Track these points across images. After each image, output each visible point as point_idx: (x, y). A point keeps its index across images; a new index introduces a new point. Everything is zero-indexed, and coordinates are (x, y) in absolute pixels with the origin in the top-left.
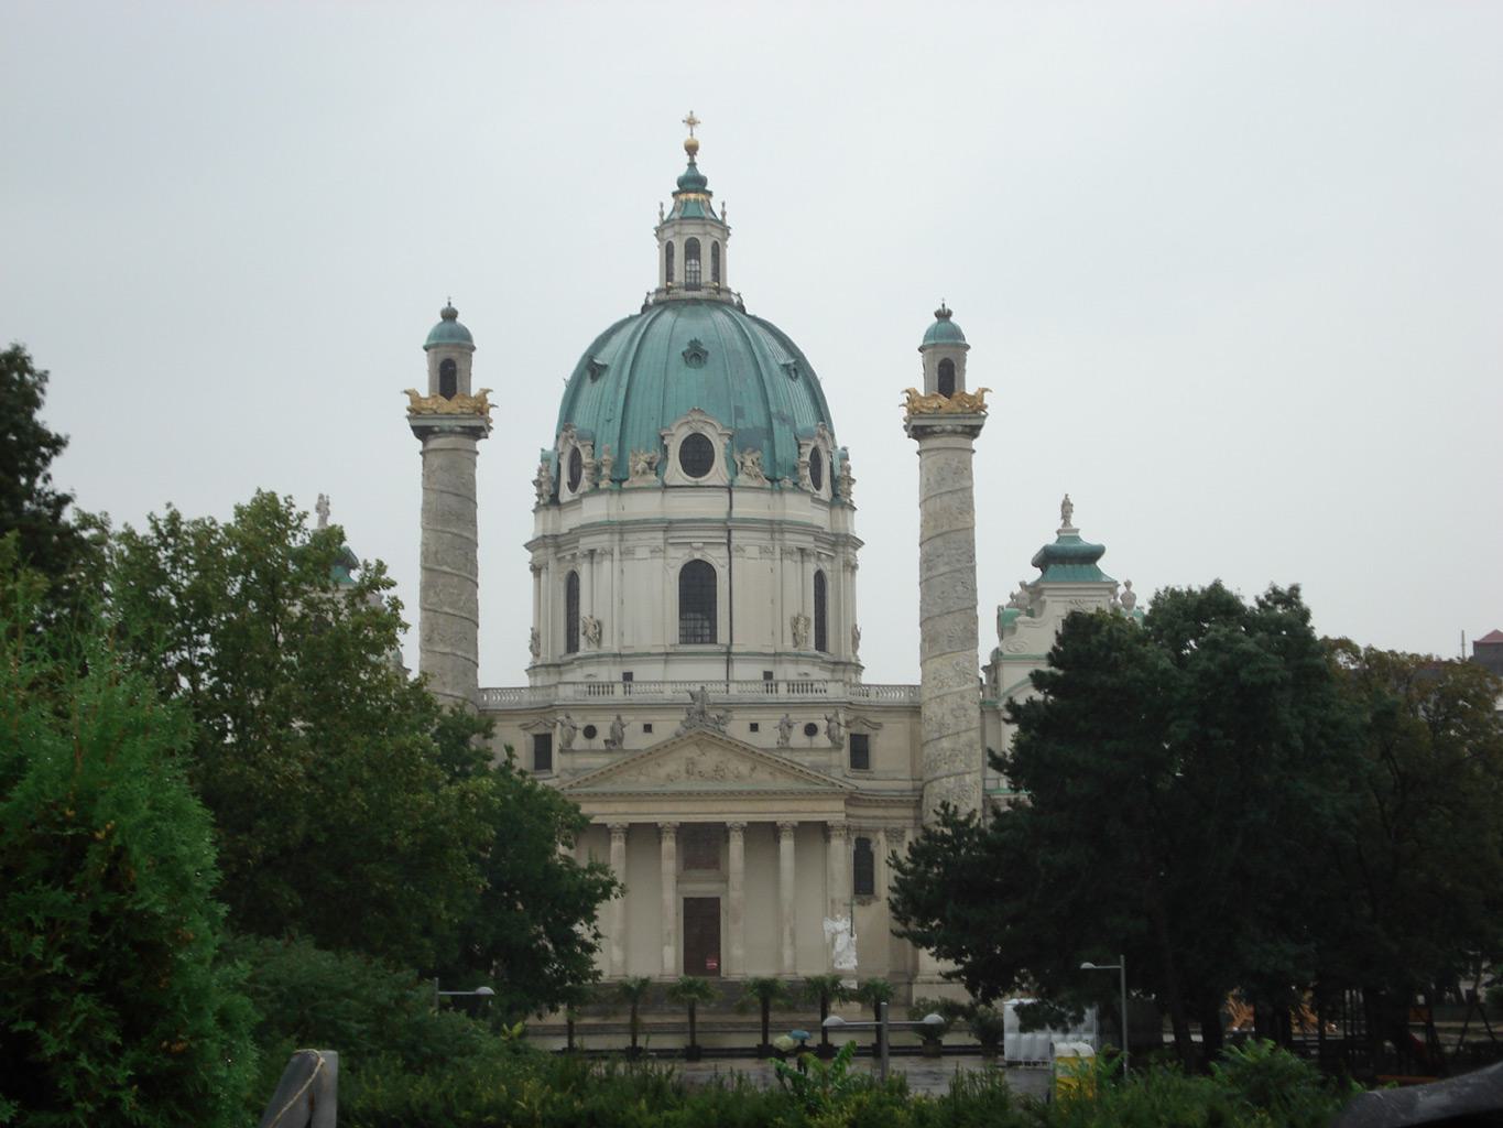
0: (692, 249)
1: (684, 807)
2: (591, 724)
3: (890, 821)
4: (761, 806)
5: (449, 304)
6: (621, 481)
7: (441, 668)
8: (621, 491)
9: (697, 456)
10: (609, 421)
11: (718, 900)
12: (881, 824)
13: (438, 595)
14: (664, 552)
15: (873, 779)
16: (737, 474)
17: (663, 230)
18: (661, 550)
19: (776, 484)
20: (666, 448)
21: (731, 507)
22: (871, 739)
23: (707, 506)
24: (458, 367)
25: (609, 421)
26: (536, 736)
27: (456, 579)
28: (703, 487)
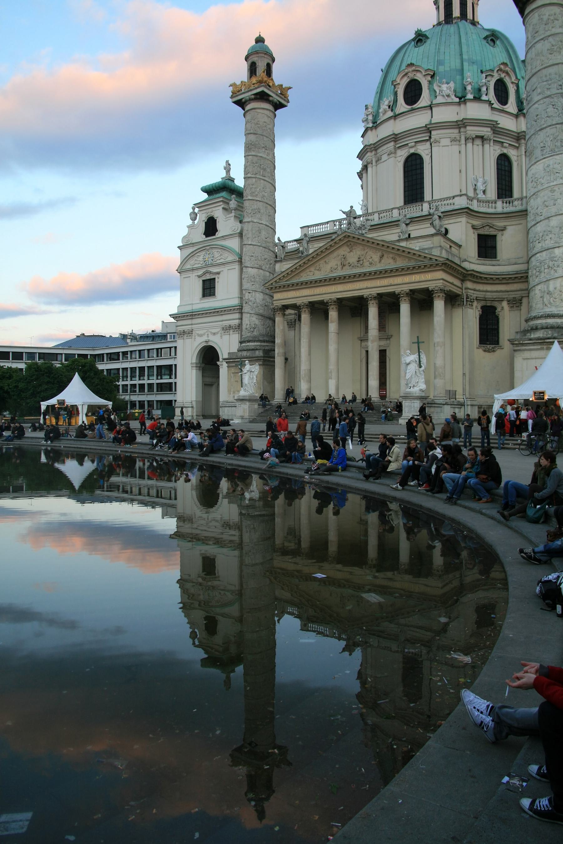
1: (340, 288)
3: (509, 293)
4: (385, 282)
6: (376, 122)
7: (247, 230)
11: (385, 350)
12: (505, 295)
14: (395, 153)
15: (499, 265)
16: (436, 97)
19: (463, 100)
20: (396, 94)
21: (432, 117)
22: (498, 238)
24: (257, 64)
27: (254, 180)
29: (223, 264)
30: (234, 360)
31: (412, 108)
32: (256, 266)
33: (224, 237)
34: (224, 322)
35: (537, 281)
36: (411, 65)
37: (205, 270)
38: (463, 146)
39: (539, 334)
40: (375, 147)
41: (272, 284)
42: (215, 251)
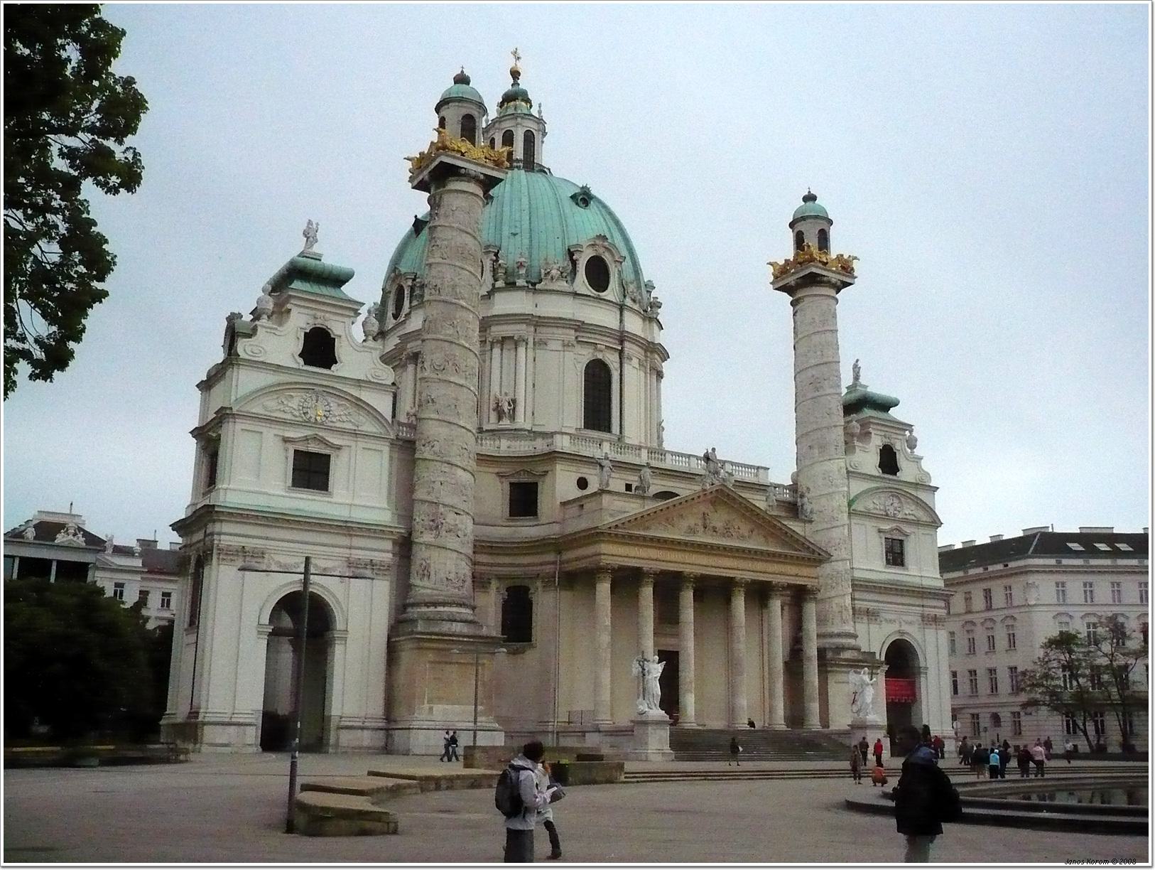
0: (529, 139)
1: (704, 560)
2: (584, 476)
4: (759, 566)
5: (462, 72)
6: (534, 284)
8: (536, 291)
9: (598, 274)
10: (517, 234)
13: (457, 327)
16: (625, 296)
17: (500, 122)
18: (573, 345)
20: (574, 263)
21: (621, 321)
23: (607, 318)
25: (515, 235)
26: (511, 484)
28: (604, 300)
29: (355, 434)
30: (440, 637)
31: (599, 295)
32: (469, 468)
33: (359, 383)
34: (353, 551)
35: (833, 593)
36: (604, 238)
37: (314, 433)
38: (648, 375)
39: (847, 655)
40: (537, 322)
41: (610, 528)
42: (330, 399)
